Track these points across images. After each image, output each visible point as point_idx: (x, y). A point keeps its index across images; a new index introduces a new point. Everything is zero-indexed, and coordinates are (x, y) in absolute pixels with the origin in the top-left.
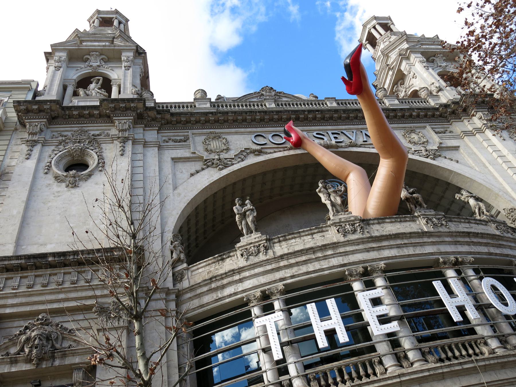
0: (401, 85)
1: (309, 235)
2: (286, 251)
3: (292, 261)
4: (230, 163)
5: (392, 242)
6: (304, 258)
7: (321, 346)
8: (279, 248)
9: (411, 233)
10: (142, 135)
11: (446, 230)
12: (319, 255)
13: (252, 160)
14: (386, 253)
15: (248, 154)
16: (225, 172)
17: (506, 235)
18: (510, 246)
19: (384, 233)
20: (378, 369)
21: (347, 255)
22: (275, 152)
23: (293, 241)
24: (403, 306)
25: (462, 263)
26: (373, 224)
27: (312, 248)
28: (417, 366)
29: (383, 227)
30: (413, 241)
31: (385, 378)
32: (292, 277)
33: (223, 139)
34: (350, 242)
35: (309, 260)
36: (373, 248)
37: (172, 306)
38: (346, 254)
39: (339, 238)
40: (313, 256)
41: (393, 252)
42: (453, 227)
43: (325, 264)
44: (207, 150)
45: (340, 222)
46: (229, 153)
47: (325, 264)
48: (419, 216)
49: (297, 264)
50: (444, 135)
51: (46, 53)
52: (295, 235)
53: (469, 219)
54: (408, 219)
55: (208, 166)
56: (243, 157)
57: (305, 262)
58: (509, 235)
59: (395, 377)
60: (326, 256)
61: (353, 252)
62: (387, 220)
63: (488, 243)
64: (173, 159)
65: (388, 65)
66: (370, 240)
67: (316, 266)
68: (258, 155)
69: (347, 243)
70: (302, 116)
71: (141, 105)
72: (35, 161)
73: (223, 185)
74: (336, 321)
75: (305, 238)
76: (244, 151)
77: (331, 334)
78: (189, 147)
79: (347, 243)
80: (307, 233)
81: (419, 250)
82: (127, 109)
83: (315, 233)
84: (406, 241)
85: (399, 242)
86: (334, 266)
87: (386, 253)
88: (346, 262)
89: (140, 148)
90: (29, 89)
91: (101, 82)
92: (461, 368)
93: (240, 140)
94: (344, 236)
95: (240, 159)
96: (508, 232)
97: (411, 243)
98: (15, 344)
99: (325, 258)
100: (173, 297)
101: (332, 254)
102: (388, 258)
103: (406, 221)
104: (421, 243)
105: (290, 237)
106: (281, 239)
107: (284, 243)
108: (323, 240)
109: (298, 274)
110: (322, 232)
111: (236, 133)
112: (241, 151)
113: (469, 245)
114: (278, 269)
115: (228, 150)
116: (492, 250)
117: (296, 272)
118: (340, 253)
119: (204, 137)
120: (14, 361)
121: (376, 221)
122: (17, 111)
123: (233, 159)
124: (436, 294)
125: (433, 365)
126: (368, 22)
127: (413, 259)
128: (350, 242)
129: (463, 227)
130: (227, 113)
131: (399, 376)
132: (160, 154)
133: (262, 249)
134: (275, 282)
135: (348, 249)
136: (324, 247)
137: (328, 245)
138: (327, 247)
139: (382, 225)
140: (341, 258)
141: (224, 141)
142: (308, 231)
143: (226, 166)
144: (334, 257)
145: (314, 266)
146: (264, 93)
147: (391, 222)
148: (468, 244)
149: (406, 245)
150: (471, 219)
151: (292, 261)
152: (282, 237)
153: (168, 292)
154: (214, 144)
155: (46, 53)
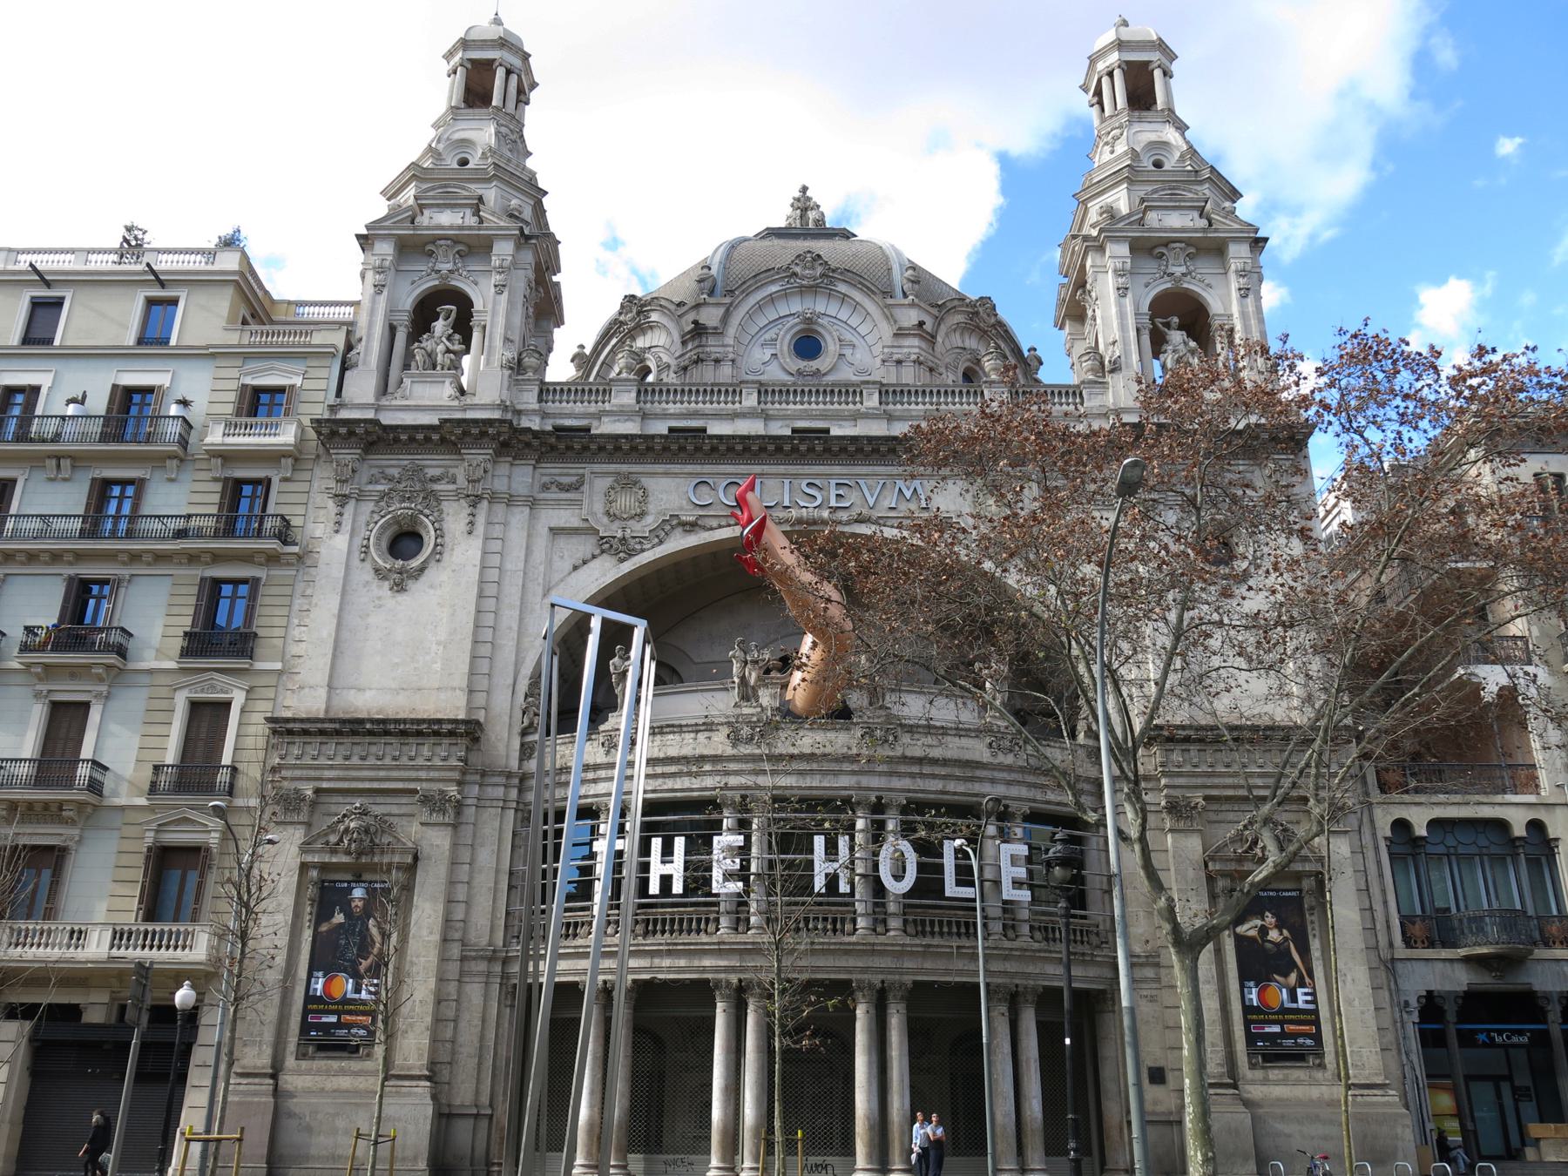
4: (638, 547)
6: (673, 769)
7: (651, 892)
10: (506, 480)
13: (679, 542)
15: (673, 528)
16: (627, 567)
22: (720, 527)
27: (685, 758)
30: (826, 766)
37: (514, 794)
43: (696, 783)
44: (608, 513)
46: (643, 522)
47: (696, 783)
51: (359, 237)
55: (603, 552)
57: (673, 775)
64: (551, 529)
67: (684, 783)
70: (787, 448)
71: (505, 429)
72: (347, 536)
74: (676, 869)
77: (666, 881)
78: (577, 503)
82: (483, 434)
84: (815, 766)
89: (500, 509)
90: (334, 355)
91: (453, 315)
93: (670, 491)
94: (734, 746)
98: (334, 832)
100: (516, 781)
116: (952, 786)
119: (609, 481)
120: (334, 852)
122: (319, 433)
124: (811, 851)
126: (1102, 53)
127: (815, 792)
130: (653, 437)
132: (532, 517)
136: (702, 759)
140: (718, 778)
143: (631, 554)
146: (798, 270)
148: (912, 776)
153: (509, 775)
154: (625, 501)
155: (359, 237)
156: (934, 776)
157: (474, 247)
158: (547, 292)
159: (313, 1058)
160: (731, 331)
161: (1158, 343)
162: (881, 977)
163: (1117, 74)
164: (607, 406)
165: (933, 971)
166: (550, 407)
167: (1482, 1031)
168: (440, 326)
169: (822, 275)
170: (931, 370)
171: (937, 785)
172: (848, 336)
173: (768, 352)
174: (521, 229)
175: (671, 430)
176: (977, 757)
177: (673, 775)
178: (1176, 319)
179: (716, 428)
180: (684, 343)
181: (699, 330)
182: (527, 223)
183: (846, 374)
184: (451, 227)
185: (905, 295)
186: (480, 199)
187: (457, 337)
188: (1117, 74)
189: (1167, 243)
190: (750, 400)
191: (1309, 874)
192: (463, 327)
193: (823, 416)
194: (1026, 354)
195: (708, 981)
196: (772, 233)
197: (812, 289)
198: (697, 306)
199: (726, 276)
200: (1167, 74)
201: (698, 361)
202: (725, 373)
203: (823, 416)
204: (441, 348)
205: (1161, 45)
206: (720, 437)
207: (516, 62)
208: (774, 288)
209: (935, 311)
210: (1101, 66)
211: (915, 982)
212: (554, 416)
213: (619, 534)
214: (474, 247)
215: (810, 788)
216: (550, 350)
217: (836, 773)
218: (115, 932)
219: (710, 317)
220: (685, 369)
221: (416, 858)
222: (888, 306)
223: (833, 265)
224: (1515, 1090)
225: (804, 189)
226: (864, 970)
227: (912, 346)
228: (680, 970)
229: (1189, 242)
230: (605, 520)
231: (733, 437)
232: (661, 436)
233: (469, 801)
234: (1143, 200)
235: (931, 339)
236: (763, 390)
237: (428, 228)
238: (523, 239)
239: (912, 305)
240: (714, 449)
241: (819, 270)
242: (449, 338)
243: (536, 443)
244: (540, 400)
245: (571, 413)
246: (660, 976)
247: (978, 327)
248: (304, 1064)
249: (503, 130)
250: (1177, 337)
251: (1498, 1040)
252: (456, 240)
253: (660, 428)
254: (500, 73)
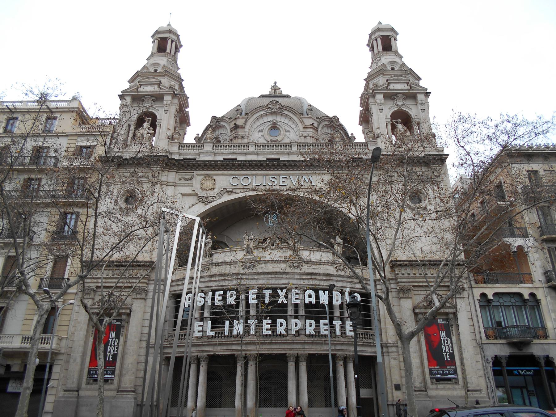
3: (217, 279)
4: (212, 200)
6: (222, 278)
13: (226, 198)
23: (222, 266)
27: (226, 274)
30: (277, 276)
32: (215, 286)
44: (201, 188)
46: (214, 191)
57: (222, 280)
70: (265, 165)
73: (207, 213)
78: (191, 185)
91: (150, 121)
93: (223, 180)
114: (210, 281)
115: (213, 189)
119: (202, 177)
130: (218, 161)
133: (207, 269)
134: (208, 287)
136: (233, 274)
143: (209, 202)
146: (270, 106)
148: (308, 279)
151: (217, 279)
154: (208, 184)
156: (316, 279)
157: (158, 98)
158: (184, 114)
159: (92, 384)
160: (247, 127)
161: (394, 127)
162: (297, 352)
163: (379, 40)
164: (202, 151)
165: (316, 350)
166: (182, 152)
167: (515, 370)
168: (146, 125)
169: (279, 108)
170: (317, 140)
171: (318, 283)
172: (288, 128)
173: (261, 134)
174: (174, 92)
175: (224, 159)
176: (331, 272)
177: (222, 280)
178: (400, 120)
179: (240, 158)
180: (231, 131)
181: (236, 127)
182: (176, 90)
183: (287, 141)
184: (150, 91)
185: (308, 115)
186: (160, 82)
187: (151, 128)
188: (379, 40)
189: (396, 94)
190: (252, 148)
191: (451, 313)
192: (153, 125)
193: (278, 154)
194: (350, 136)
195: (234, 355)
196: (262, 96)
197: (274, 113)
198: (236, 119)
199: (246, 109)
200: (395, 39)
201: (236, 137)
202: (246, 140)
203: (278, 154)
204: (146, 132)
205: (392, 30)
206: (241, 161)
207: (175, 38)
208: (262, 113)
209: (318, 120)
210: (373, 37)
211: (309, 354)
212: (184, 154)
213: (205, 195)
214: (158, 98)
216: (185, 134)
217: (280, 279)
218: (23, 338)
219: (240, 122)
220: (231, 140)
221: (131, 311)
222: (301, 118)
223: (283, 104)
224: (528, 391)
225: (275, 83)
226: (290, 350)
227: (310, 131)
228: (224, 351)
229: (404, 94)
230: (201, 190)
231: (246, 161)
232: (220, 161)
233: (150, 291)
234: (387, 80)
235: (316, 129)
236: (257, 145)
237: (142, 92)
238: (174, 95)
239: (310, 118)
240: (239, 165)
241: (278, 106)
242: (149, 129)
243: (177, 164)
244: (179, 149)
245: (189, 154)
246: (217, 353)
247: (333, 126)
248: (89, 387)
249: (170, 60)
250: (400, 126)
251: (521, 373)
252: (152, 96)
253: (221, 158)
254: (170, 41)
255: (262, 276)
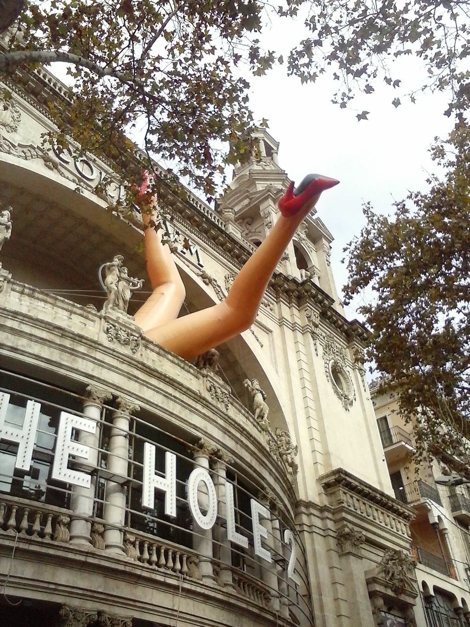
0: (248, 223)
1: (66, 310)
2: (24, 310)
3: (26, 329)
4: (7, 148)
5: (162, 385)
6: (44, 335)
8: (18, 300)
9: (188, 389)
11: (224, 410)
12: (67, 343)
14: (148, 394)
17: (272, 454)
18: (271, 470)
19: (160, 370)
20: (62, 531)
21: (102, 366)
23: (42, 304)
24: (192, 456)
25: (220, 457)
26: (152, 350)
28: (113, 553)
29: (160, 361)
31: (68, 549)
33: (16, 112)
34: (115, 353)
35: (49, 341)
36: (138, 378)
38: (101, 364)
39: (104, 339)
40: (58, 340)
41: (158, 399)
42: (232, 412)
45: (115, 321)
48: (207, 376)
49: (30, 337)
50: (264, 307)
52: (49, 300)
53: (249, 415)
54: (192, 371)
56: (28, 154)
57: (43, 341)
58: (275, 457)
59: (81, 553)
60: (76, 351)
61: (111, 368)
62: (170, 357)
63: (255, 454)
65: (248, 191)
66: (140, 366)
68: (49, 168)
69: (111, 352)
75: (60, 310)
76: (34, 148)
79: (111, 352)
80: (66, 306)
81: (185, 414)
83: (75, 313)
84: (177, 394)
85: (170, 390)
86: (77, 370)
87: (148, 394)
88: (95, 374)
92: (163, 580)
95: (23, 155)
96: (275, 454)
97: (182, 401)
99: (73, 352)
101: (84, 354)
102: (148, 402)
103: (189, 372)
104: (192, 407)
105: (41, 296)
106: (26, 291)
107: (27, 298)
108: (82, 329)
109: (23, 351)
110: (87, 318)
111: (39, 119)
112: (31, 146)
113: (237, 443)
115: (14, 130)
117: (23, 346)
118: (95, 359)
121: (157, 349)
123: (14, 146)
125: (132, 561)
128: (115, 353)
129: (240, 419)
131: (87, 554)
135: (108, 359)
136: (79, 338)
137: (86, 339)
138: (84, 340)
139: (161, 358)
140: (91, 365)
141: (16, 115)
142: (69, 304)
144: (84, 359)
145: (51, 353)
147: (173, 362)
149: (175, 399)
150: (251, 416)
152: (30, 289)
177: (43, 341)
215: (171, 414)
255: (154, 382)
